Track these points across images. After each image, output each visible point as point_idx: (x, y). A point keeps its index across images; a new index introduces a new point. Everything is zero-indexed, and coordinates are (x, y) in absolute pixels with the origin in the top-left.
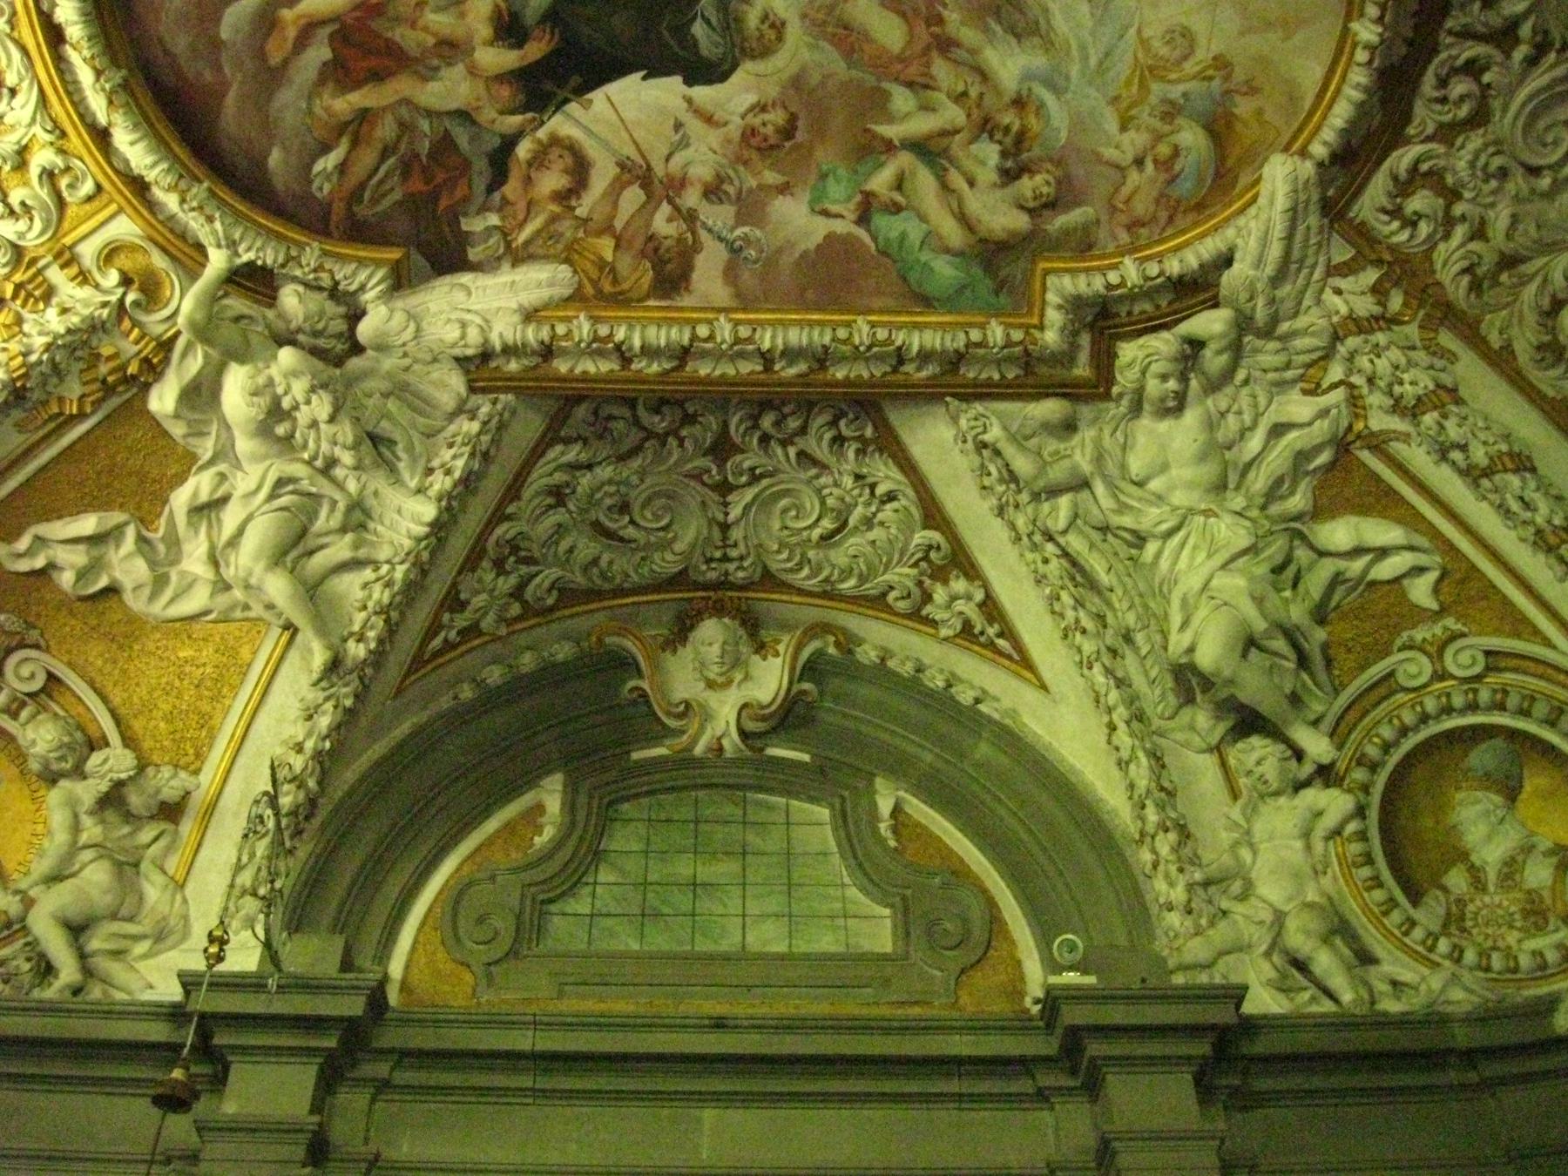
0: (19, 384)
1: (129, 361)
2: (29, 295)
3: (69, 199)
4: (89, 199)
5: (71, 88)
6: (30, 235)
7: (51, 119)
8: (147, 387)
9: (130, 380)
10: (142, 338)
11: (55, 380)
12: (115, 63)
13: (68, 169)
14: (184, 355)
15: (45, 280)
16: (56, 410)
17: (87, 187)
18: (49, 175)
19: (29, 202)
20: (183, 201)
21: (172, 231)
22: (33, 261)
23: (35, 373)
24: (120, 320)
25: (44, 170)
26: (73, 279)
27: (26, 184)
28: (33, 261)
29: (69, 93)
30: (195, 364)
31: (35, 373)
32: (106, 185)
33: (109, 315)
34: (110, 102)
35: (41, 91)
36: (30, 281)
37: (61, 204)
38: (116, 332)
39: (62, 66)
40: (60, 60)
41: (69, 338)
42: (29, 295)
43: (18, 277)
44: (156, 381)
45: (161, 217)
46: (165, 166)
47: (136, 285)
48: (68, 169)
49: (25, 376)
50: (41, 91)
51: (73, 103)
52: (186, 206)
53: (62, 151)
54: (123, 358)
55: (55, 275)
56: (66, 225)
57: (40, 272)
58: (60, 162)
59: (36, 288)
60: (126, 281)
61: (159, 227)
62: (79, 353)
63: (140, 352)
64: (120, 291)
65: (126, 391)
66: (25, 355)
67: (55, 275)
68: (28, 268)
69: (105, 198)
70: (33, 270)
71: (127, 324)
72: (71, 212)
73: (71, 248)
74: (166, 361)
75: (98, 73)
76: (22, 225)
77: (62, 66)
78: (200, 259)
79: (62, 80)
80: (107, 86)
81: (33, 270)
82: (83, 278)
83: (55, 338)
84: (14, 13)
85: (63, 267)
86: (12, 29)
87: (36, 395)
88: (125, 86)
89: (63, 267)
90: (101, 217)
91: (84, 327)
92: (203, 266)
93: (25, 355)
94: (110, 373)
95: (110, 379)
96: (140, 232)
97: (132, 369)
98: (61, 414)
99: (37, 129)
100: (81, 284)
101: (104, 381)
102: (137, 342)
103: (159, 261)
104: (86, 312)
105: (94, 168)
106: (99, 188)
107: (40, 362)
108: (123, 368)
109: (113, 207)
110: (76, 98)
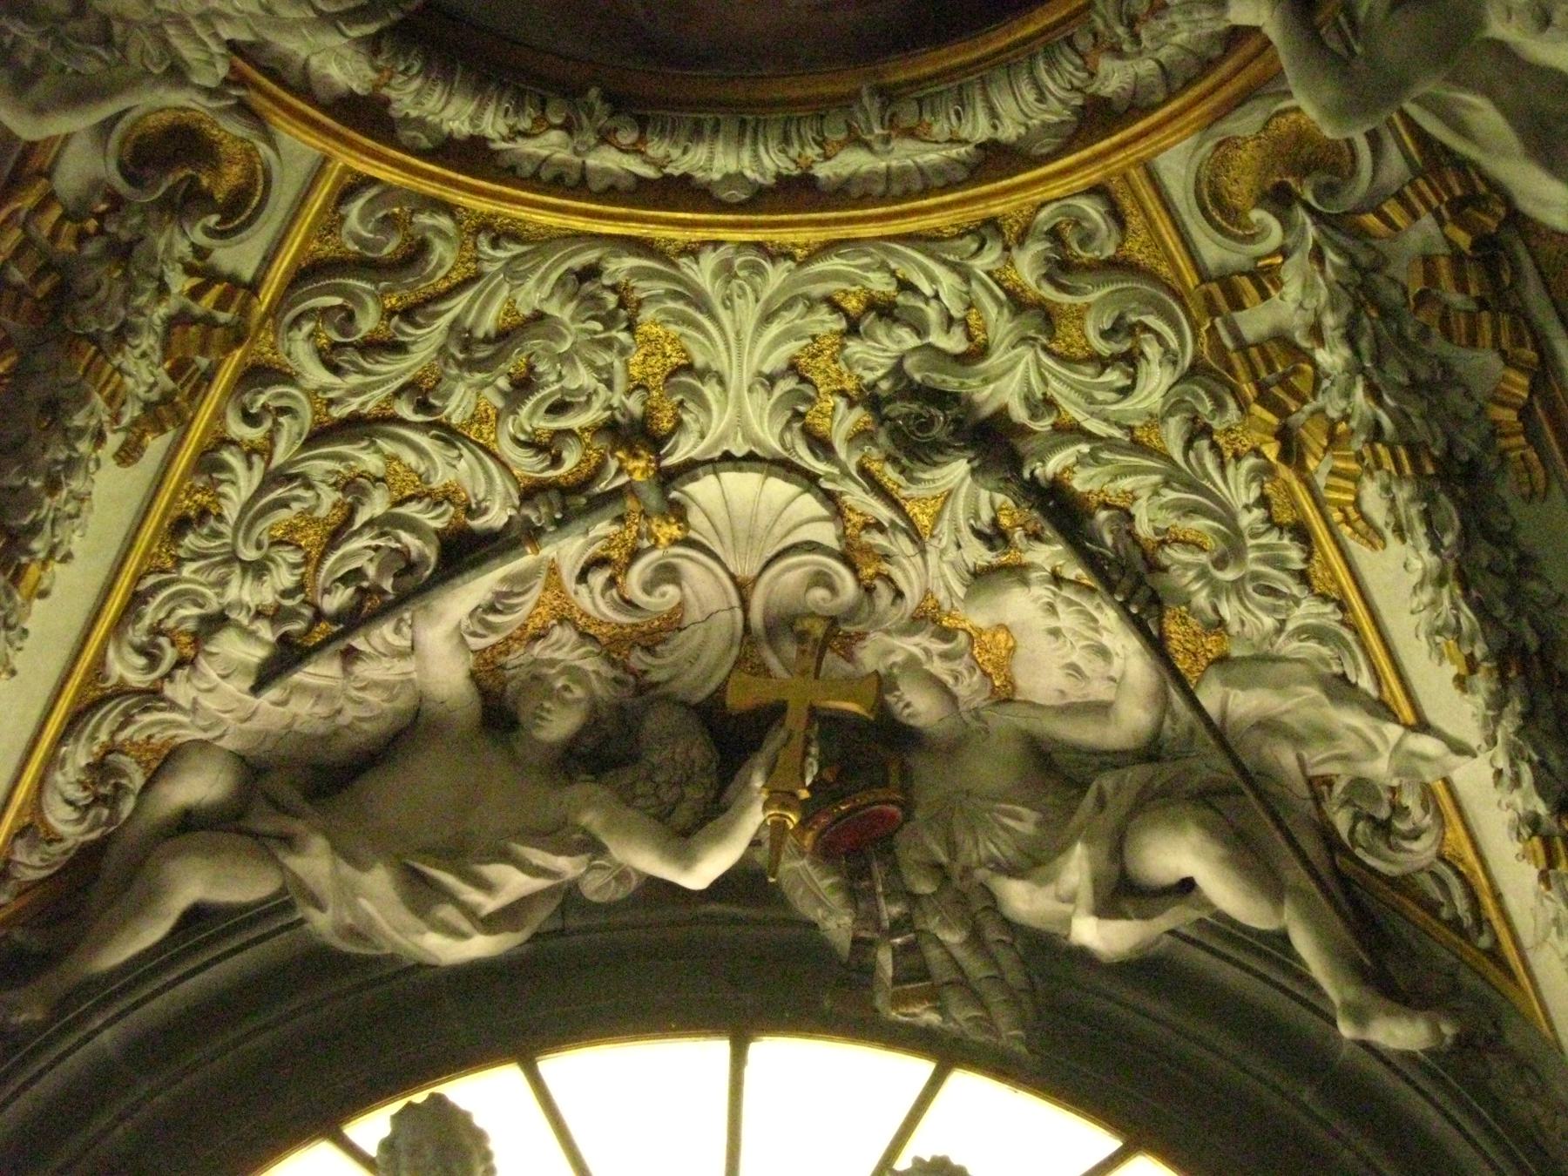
0: (1430, 470)
1: (1450, 243)
2: (1283, 381)
3: (1110, 251)
4: (1117, 215)
5: (897, 189)
6: (1174, 343)
7: (961, 236)
8: (1516, 219)
9: (1489, 252)
10: (1400, 197)
11: (1455, 397)
12: (846, 102)
13: (1055, 235)
14: (1461, 129)
15: (1259, 345)
16: (1508, 415)
17: (1092, 210)
18: (1061, 269)
19: (1107, 325)
20: (1117, 52)
21: (1188, 83)
22: (1218, 348)
23: (1420, 430)
24: (1362, 234)
25: (1049, 278)
26: (1265, 296)
27: (1080, 314)
28: (1218, 348)
29: (907, 195)
30: (1485, 115)
31: (1420, 430)
32: (1094, 175)
33: (1341, 251)
34: (911, 133)
35: (908, 238)
36: (1254, 376)
37: (1119, 266)
38: (1384, 246)
39: (856, 192)
40: (844, 194)
41: (1364, 344)
42: (1283, 381)
43: (1249, 390)
44: (1508, 200)
45: (1160, 97)
46: (1041, 65)
47: (1291, 180)
48: (1055, 235)
49: (1414, 450)
50: (908, 238)
51: (926, 192)
52: (1126, 47)
53: (1022, 239)
54: (1442, 249)
55: (1256, 321)
56: (1164, 269)
57: (1242, 346)
58: (1036, 247)
59: (1271, 368)
60: (1280, 199)
61: (1175, 105)
62: (1410, 331)
63: (1437, 214)
64: (1301, 215)
65: (1517, 272)
66: (1376, 431)
67: (1256, 321)
68: (1230, 369)
69: (1115, 184)
70: (1236, 358)
71: (1371, 220)
72: (1137, 249)
73: (1203, 276)
74: (1462, 165)
75: (856, 140)
76: (1152, 350)
77: (856, 192)
78: (1251, 47)
79: (883, 199)
80: (878, 131)
81: (1236, 358)
82: (1264, 279)
83: (1362, 370)
84: (759, 246)
85: (1238, 305)
86: (789, 256)
87: (1469, 443)
88: (888, 96)
89: (1238, 305)
90: (1153, 206)
91: (1347, 308)
92: (1268, 43)
93: (1376, 431)
94: (1462, 288)
95: (1474, 291)
96: (1191, 141)
97: (1463, 239)
98: (1525, 412)
99: (980, 265)
100: (1278, 284)
101: (1482, 303)
102: (1415, 216)
103: (1246, 123)
104: (1324, 294)
105: (1056, 189)
106: (1096, 191)
107: (1401, 418)
108: (1457, 258)
109: (1136, 175)
110: (917, 186)
